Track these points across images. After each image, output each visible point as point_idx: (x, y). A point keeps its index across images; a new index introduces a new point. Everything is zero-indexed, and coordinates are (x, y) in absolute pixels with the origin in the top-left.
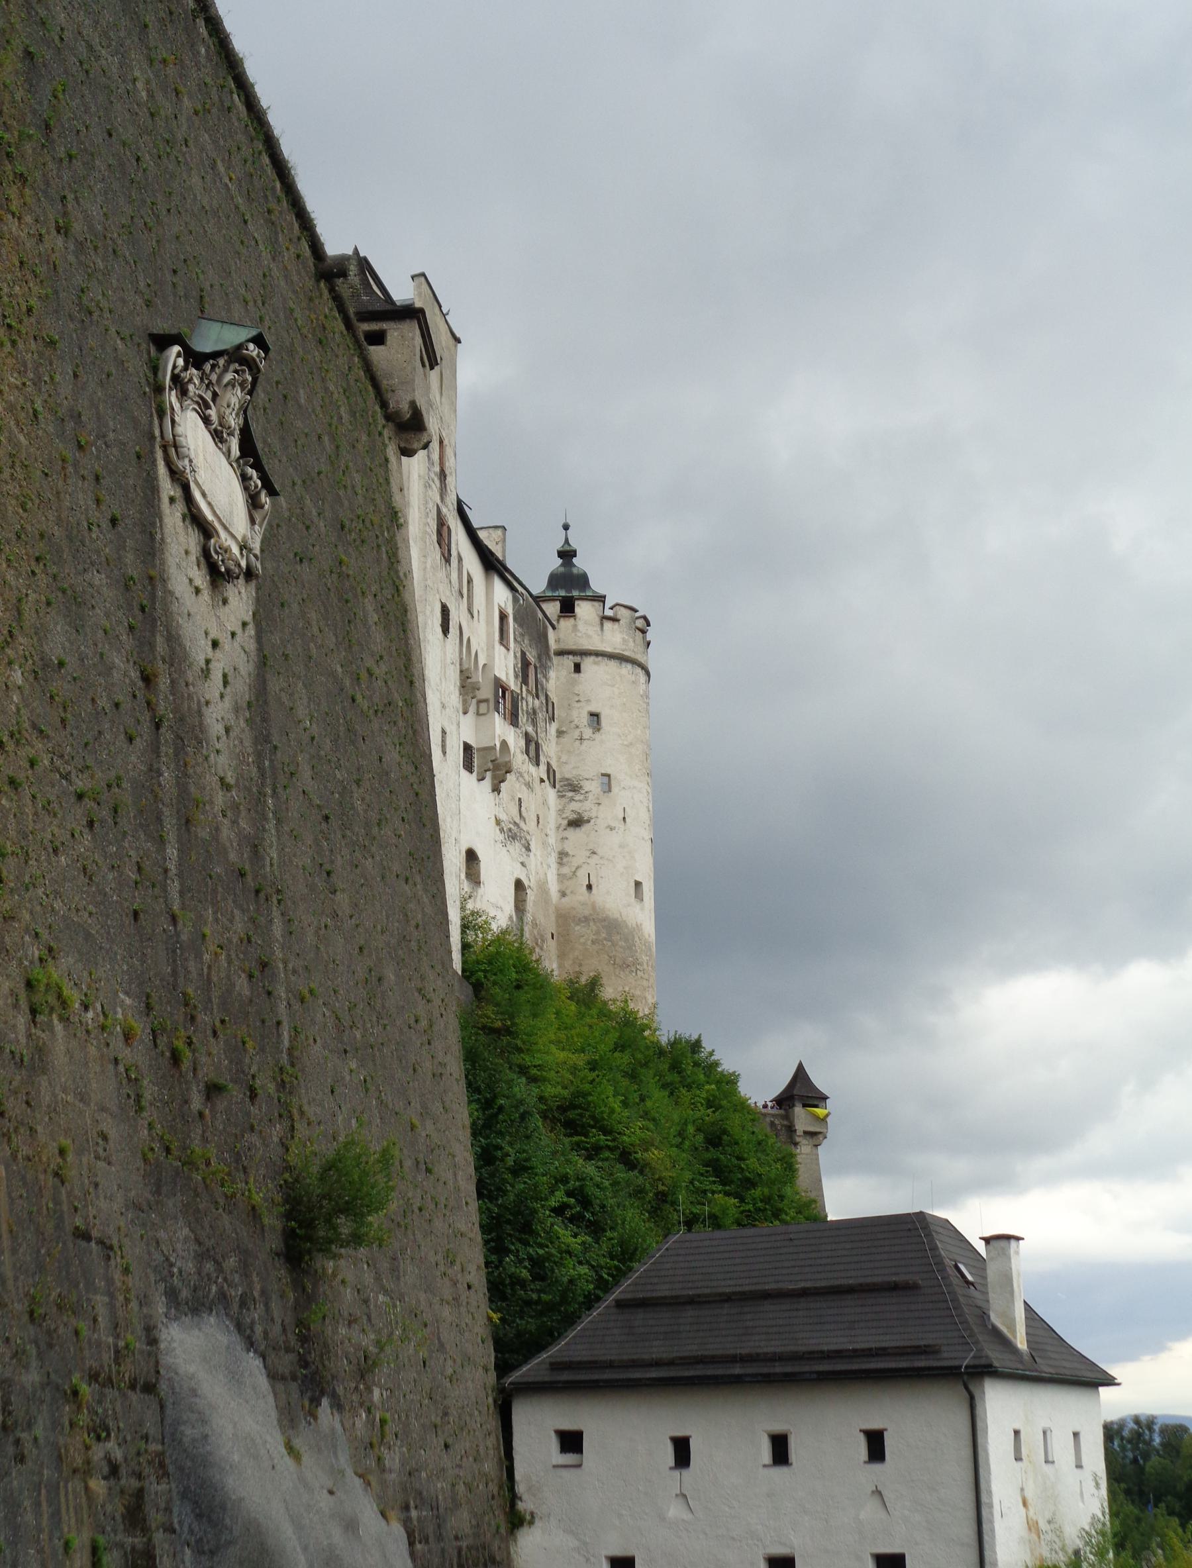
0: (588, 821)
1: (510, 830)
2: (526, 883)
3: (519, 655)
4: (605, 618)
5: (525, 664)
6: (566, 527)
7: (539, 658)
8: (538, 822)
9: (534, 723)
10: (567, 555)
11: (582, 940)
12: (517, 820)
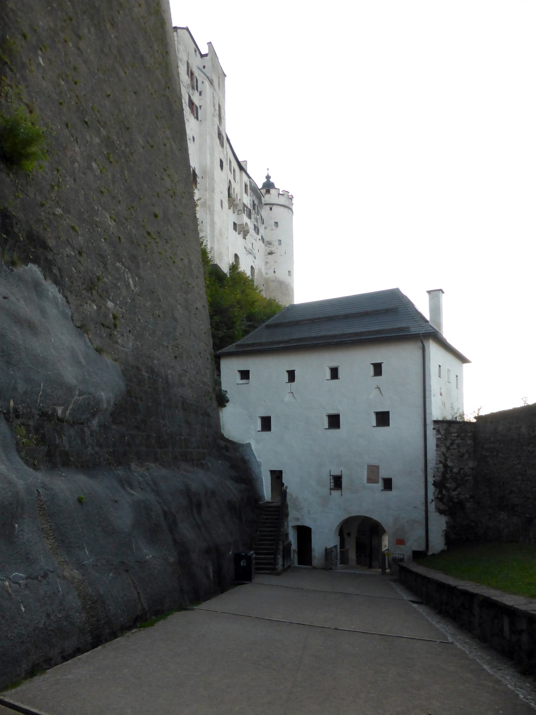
0: (274, 253)
1: (249, 251)
2: (255, 268)
3: (252, 201)
4: (279, 194)
5: (254, 205)
7: (259, 204)
8: (258, 251)
9: (257, 222)
10: (268, 177)
12: (252, 249)
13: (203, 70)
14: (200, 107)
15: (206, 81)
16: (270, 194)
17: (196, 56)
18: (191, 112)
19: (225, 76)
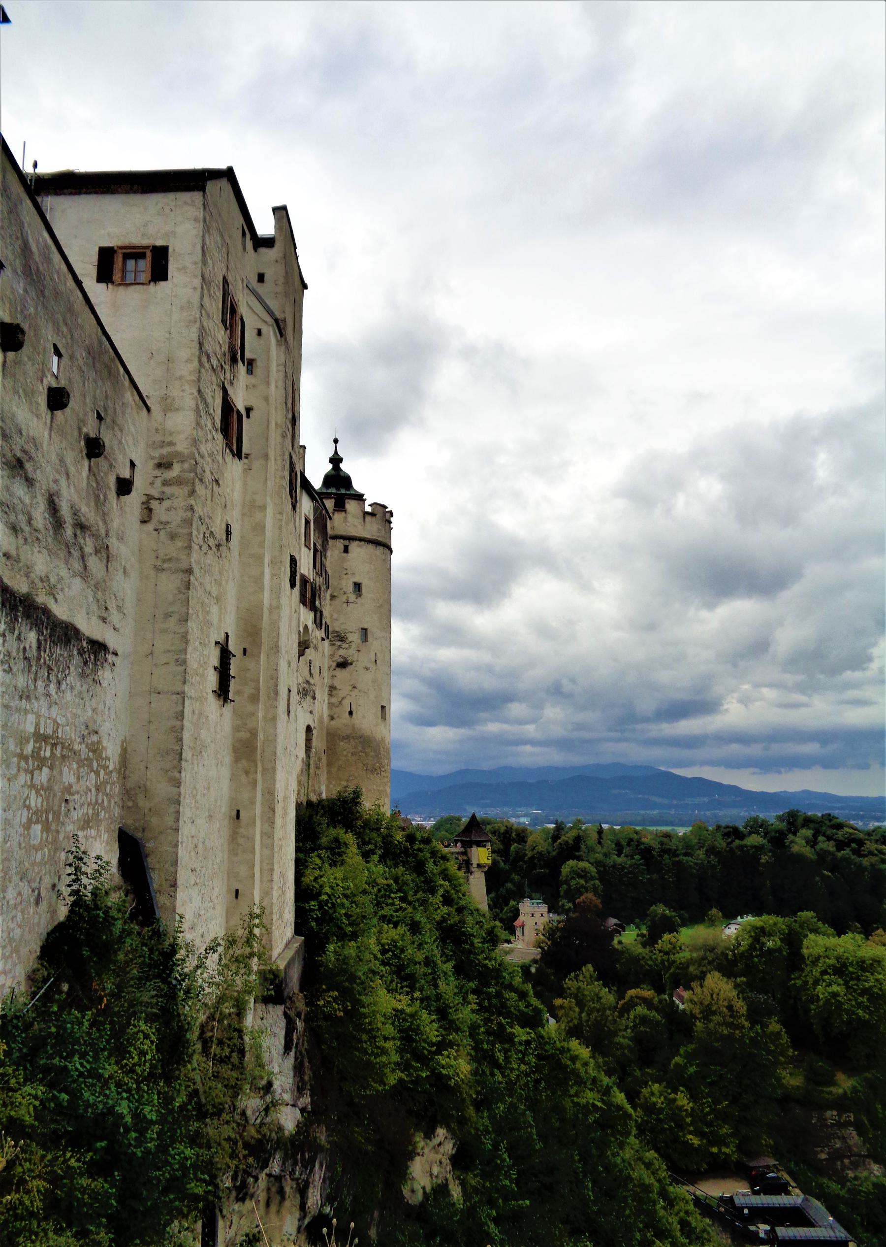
0: (351, 664)
6: (336, 441)
10: (336, 460)
11: (345, 753)
13: (260, 289)
14: (248, 410)
15: (271, 329)
16: (345, 511)
17: (244, 248)
18: (227, 444)
19: (305, 287)
